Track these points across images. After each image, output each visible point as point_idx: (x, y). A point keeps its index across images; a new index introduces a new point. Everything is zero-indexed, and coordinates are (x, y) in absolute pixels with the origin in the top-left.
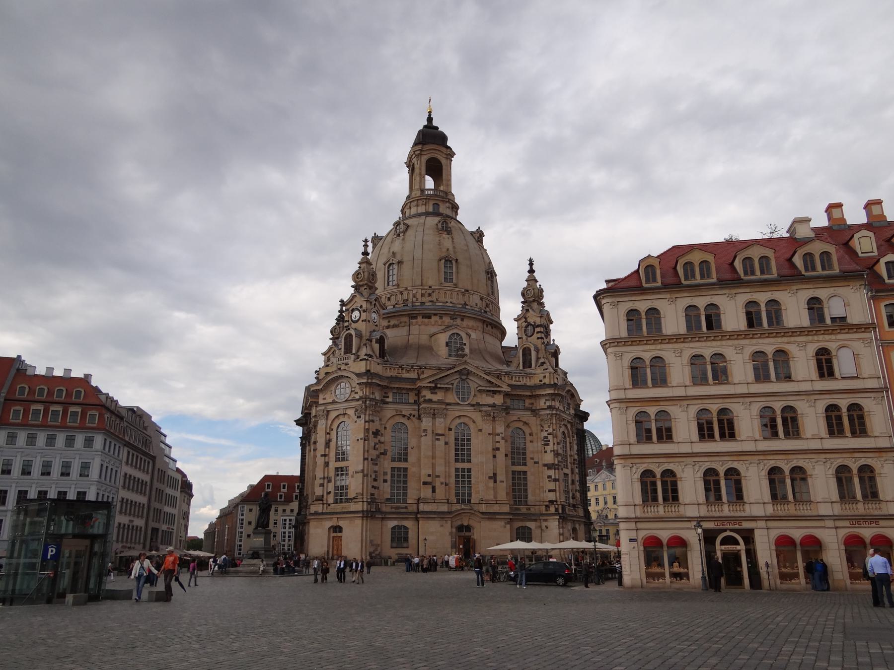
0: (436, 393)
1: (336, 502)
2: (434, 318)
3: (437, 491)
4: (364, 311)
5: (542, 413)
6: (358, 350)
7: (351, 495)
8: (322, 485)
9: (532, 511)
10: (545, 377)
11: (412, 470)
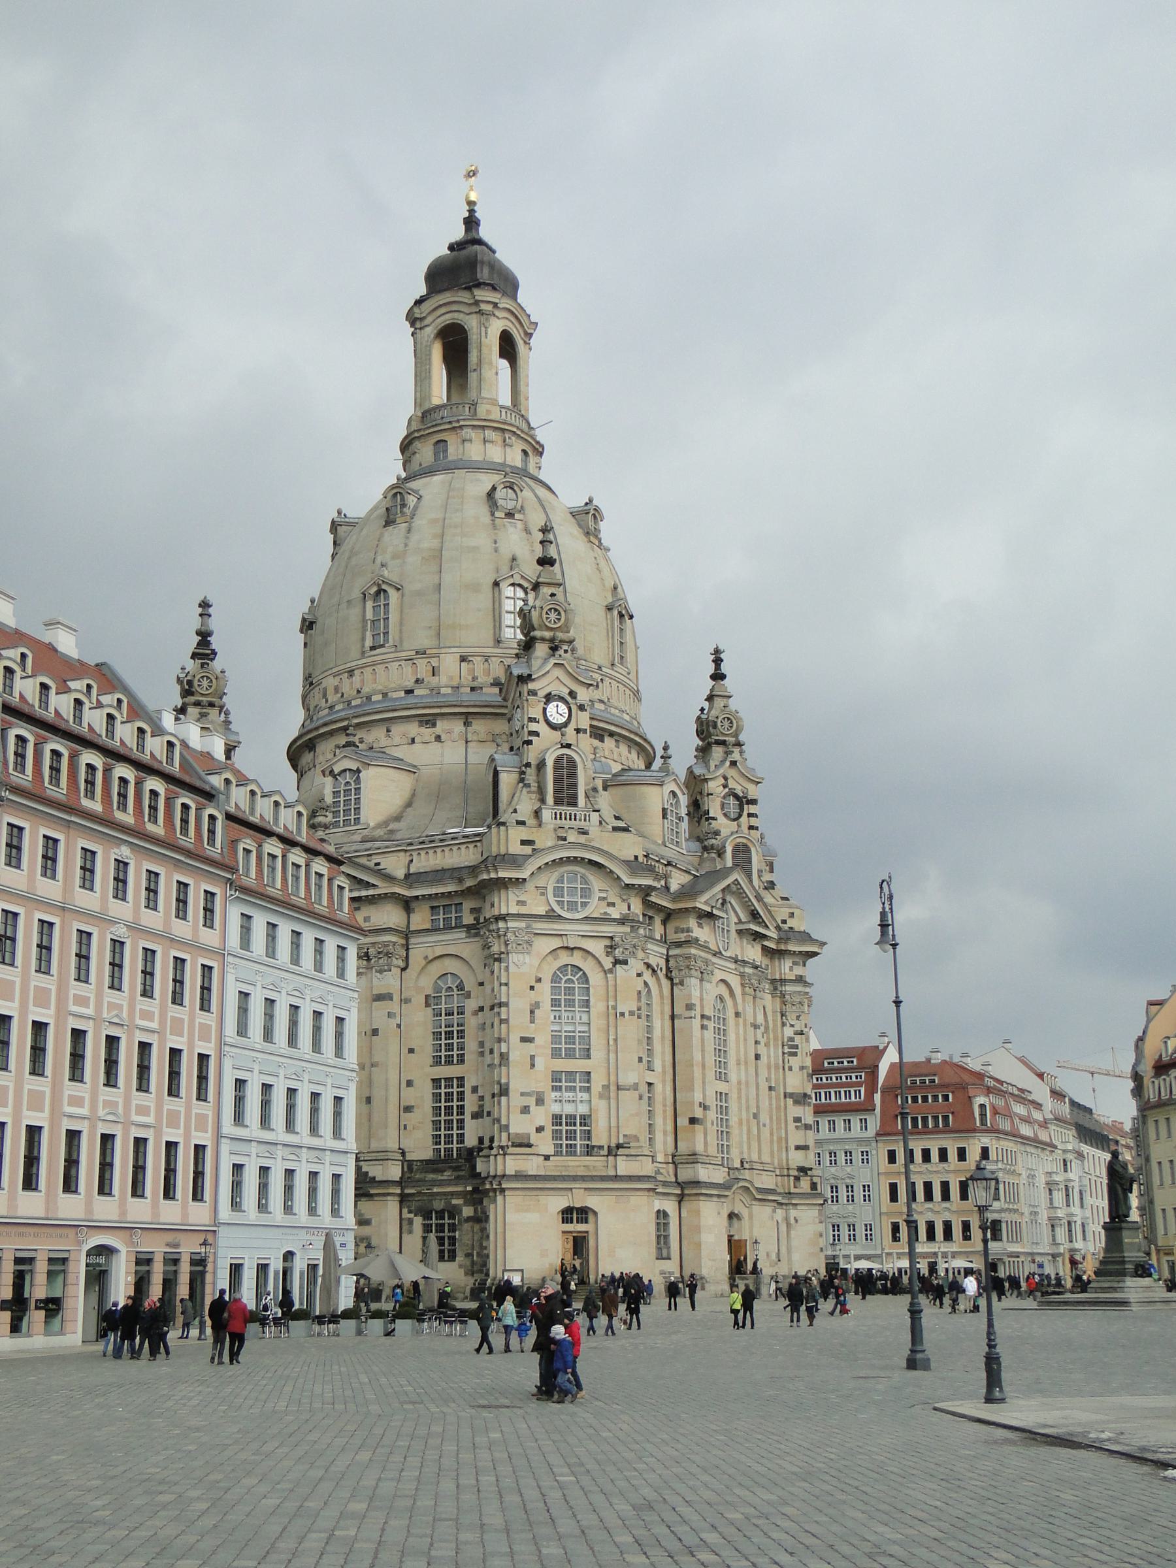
2: (609, 742)
4: (581, 708)
5: (789, 988)
8: (525, 1110)
10: (792, 915)
11: (658, 1088)
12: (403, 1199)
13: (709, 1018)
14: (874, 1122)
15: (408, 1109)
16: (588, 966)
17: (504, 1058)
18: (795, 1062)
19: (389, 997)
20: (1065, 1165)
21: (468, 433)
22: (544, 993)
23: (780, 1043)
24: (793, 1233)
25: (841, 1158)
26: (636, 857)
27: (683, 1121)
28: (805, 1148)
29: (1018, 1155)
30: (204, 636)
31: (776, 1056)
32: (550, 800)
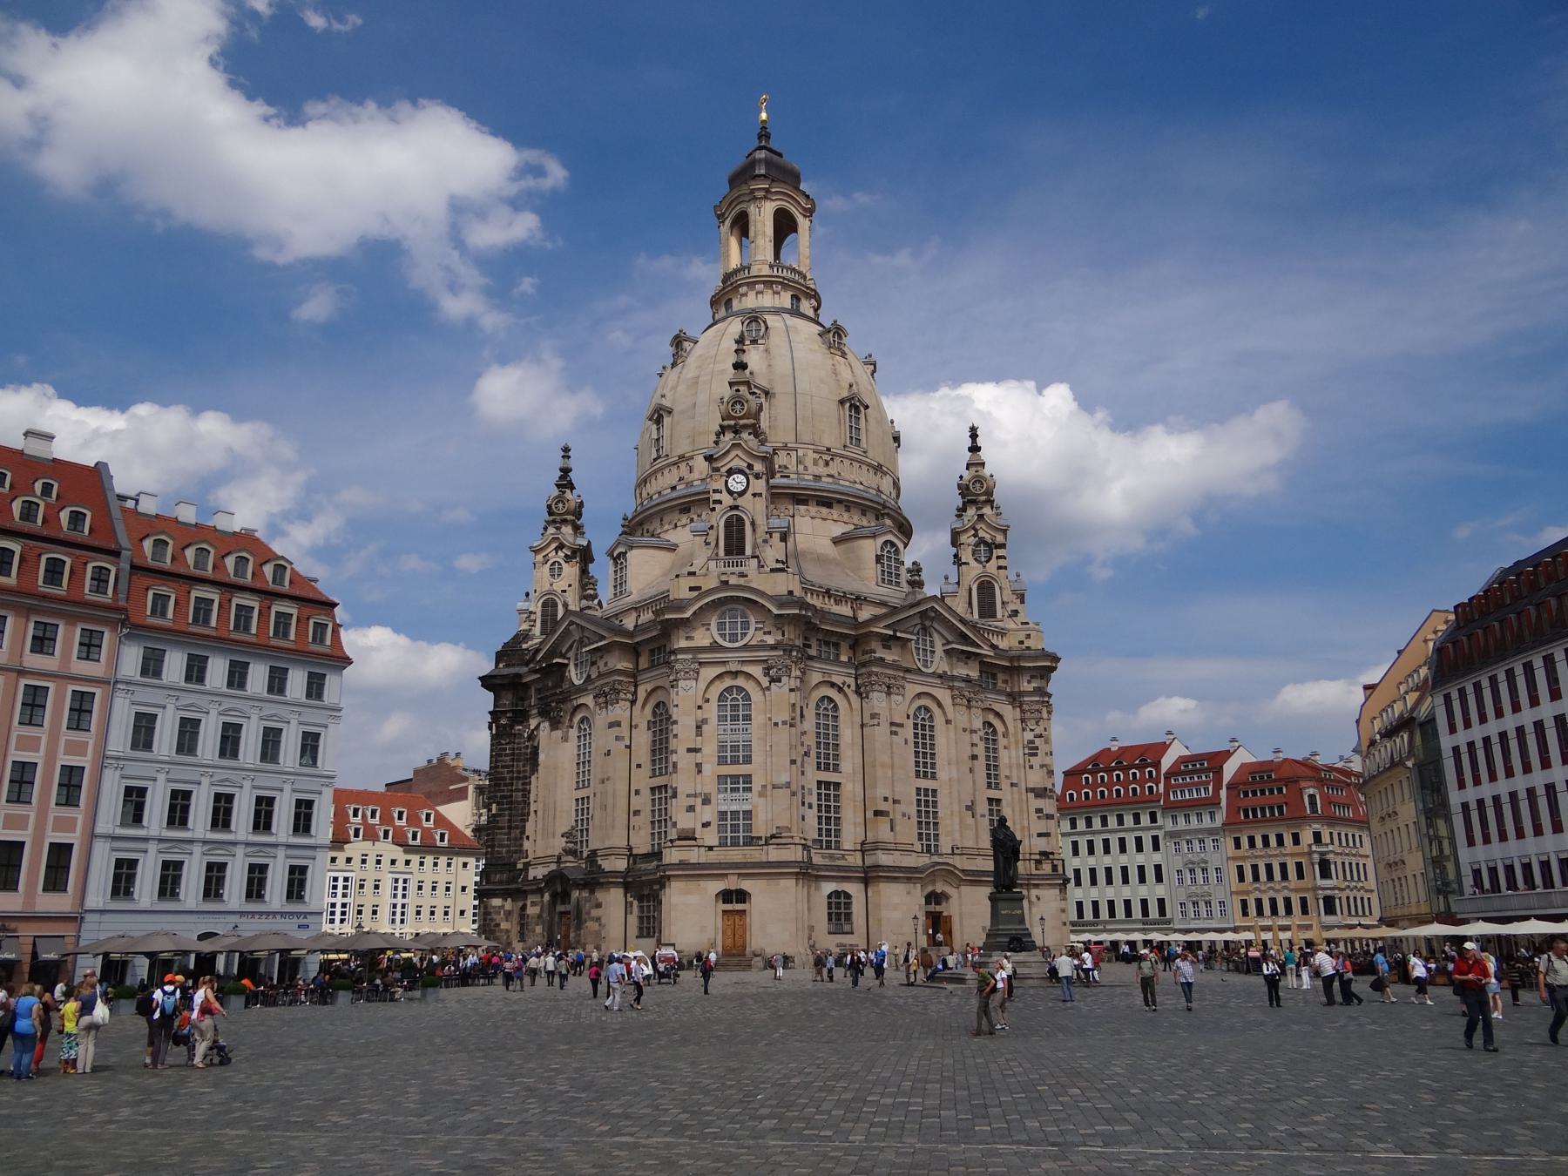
0: (889, 648)
1: (723, 844)
3: (897, 828)
4: (757, 477)
6: (755, 546)
7: (761, 828)
8: (691, 809)
10: (1028, 636)
12: (627, 887)
13: (901, 725)
14: (1220, 817)
15: (637, 813)
16: (749, 686)
17: (675, 765)
18: (1035, 761)
19: (618, 724)
21: (743, 290)
22: (712, 711)
26: (791, 593)
27: (870, 814)
28: (1047, 835)
30: (566, 471)
32: (722, 552)
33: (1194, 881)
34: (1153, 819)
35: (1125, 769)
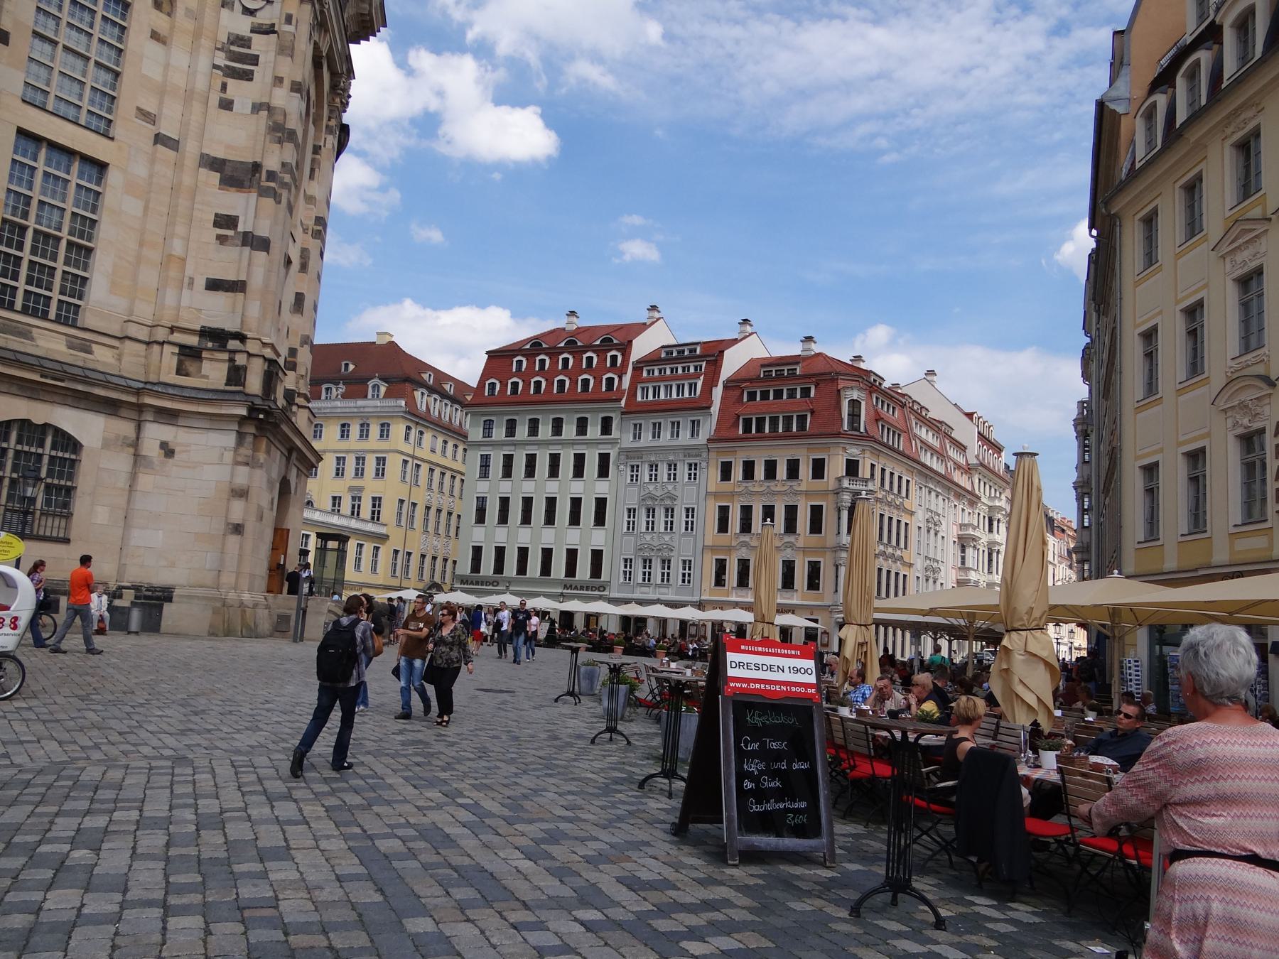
9: (102, 357)
14: (708, 427)
20: (991, 524)
23: (206, 43)
24: (146, 480)
25: (663, 472)
28: (236, 287)
29: (913, 486)
31: (191, 71)
33: (651, 526)
34: (606, 426)
35: (578, 353)
